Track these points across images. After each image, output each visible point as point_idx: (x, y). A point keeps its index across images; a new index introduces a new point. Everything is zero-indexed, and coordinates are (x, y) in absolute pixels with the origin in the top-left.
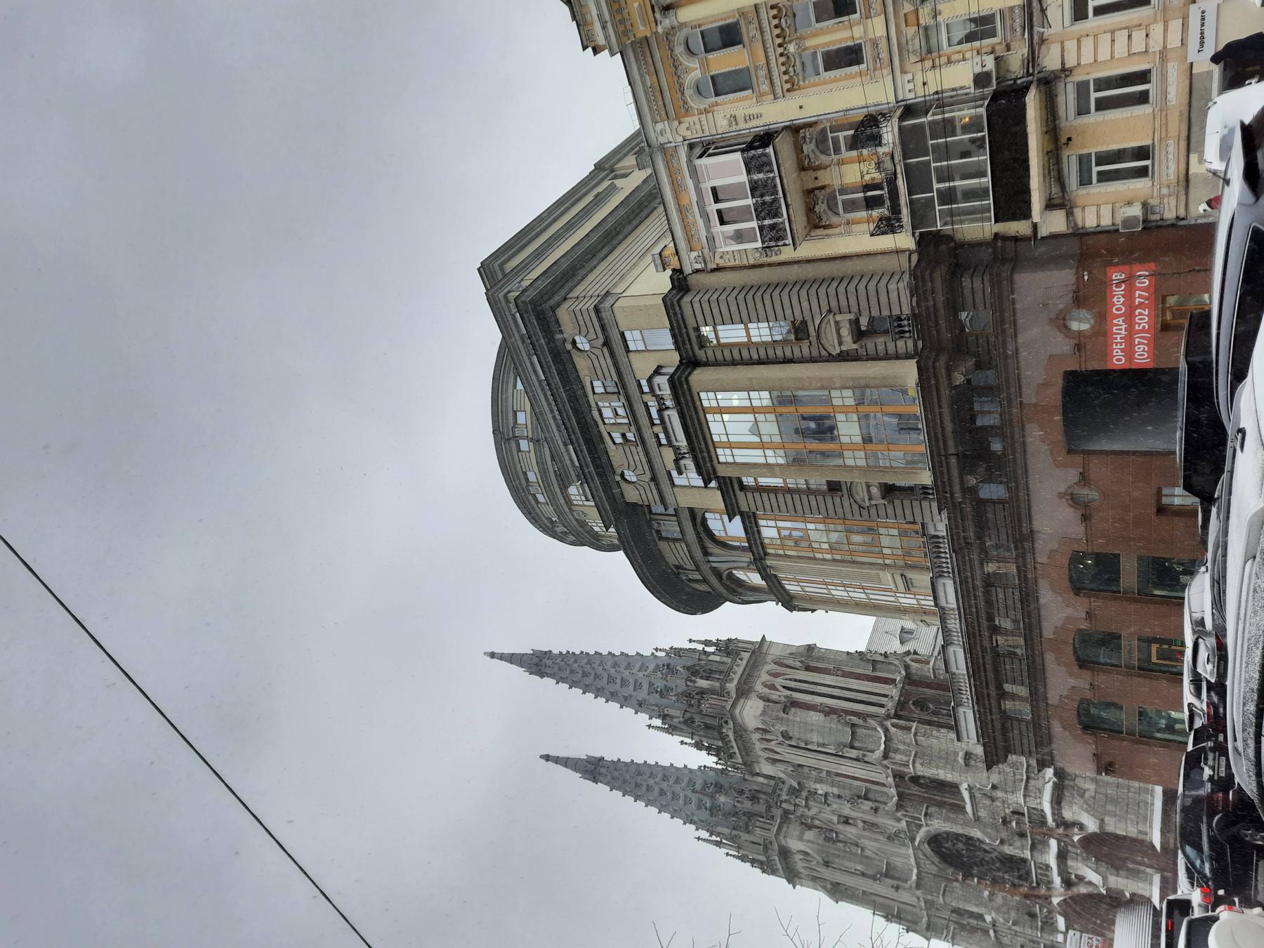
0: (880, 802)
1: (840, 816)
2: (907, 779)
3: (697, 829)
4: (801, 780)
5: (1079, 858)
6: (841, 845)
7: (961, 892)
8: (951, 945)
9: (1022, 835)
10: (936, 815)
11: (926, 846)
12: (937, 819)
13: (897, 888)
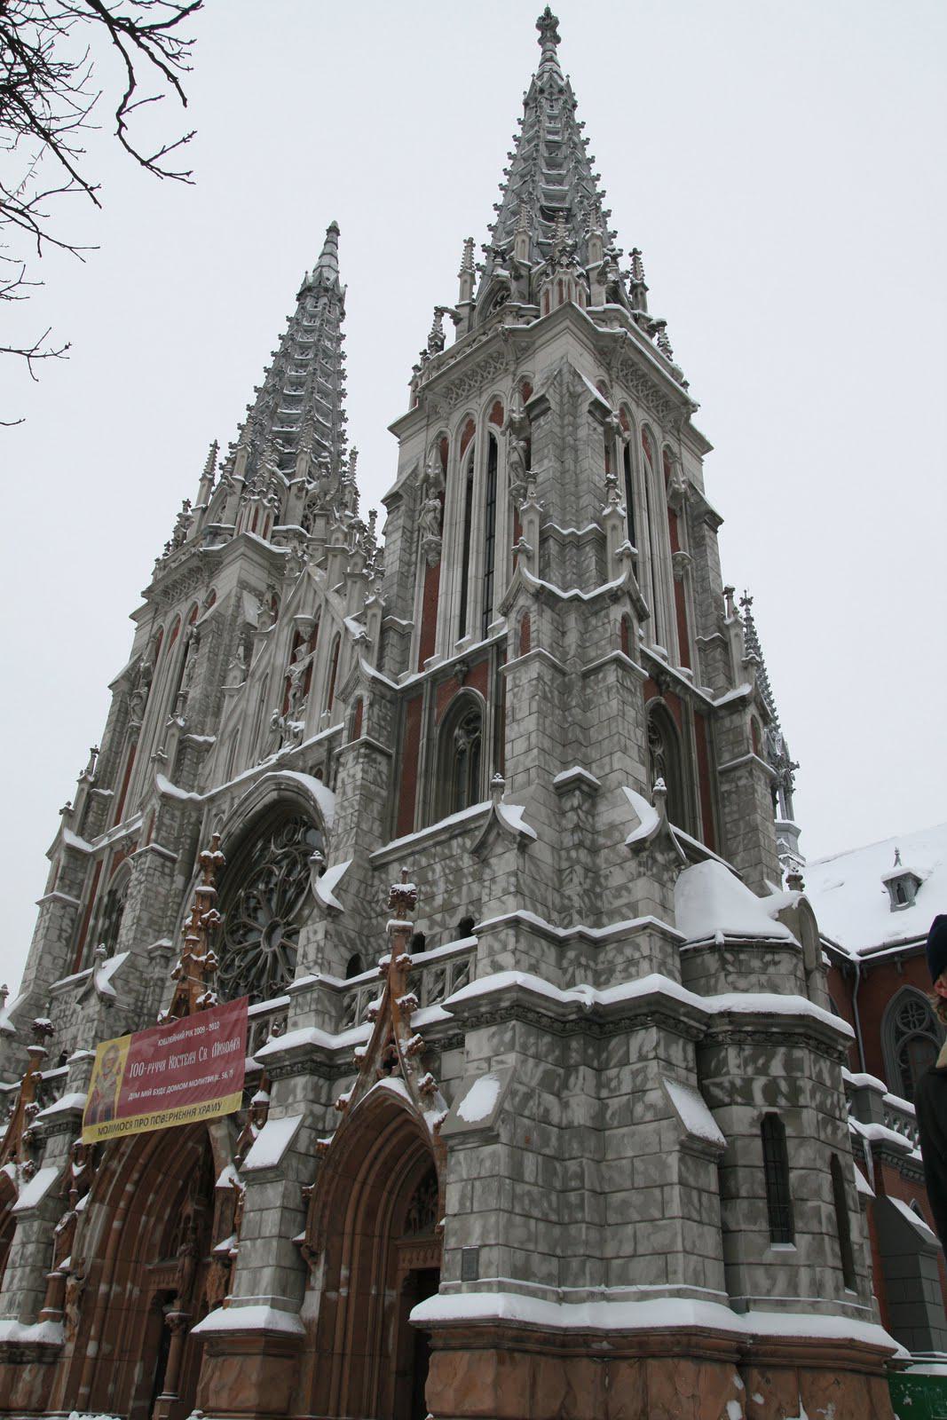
2: (462, 690)
3: (232, 446)
5: (318, 1109)
7: (163, 892)
8: (41, 897)
11: (274, 795)
12: (363, 770)
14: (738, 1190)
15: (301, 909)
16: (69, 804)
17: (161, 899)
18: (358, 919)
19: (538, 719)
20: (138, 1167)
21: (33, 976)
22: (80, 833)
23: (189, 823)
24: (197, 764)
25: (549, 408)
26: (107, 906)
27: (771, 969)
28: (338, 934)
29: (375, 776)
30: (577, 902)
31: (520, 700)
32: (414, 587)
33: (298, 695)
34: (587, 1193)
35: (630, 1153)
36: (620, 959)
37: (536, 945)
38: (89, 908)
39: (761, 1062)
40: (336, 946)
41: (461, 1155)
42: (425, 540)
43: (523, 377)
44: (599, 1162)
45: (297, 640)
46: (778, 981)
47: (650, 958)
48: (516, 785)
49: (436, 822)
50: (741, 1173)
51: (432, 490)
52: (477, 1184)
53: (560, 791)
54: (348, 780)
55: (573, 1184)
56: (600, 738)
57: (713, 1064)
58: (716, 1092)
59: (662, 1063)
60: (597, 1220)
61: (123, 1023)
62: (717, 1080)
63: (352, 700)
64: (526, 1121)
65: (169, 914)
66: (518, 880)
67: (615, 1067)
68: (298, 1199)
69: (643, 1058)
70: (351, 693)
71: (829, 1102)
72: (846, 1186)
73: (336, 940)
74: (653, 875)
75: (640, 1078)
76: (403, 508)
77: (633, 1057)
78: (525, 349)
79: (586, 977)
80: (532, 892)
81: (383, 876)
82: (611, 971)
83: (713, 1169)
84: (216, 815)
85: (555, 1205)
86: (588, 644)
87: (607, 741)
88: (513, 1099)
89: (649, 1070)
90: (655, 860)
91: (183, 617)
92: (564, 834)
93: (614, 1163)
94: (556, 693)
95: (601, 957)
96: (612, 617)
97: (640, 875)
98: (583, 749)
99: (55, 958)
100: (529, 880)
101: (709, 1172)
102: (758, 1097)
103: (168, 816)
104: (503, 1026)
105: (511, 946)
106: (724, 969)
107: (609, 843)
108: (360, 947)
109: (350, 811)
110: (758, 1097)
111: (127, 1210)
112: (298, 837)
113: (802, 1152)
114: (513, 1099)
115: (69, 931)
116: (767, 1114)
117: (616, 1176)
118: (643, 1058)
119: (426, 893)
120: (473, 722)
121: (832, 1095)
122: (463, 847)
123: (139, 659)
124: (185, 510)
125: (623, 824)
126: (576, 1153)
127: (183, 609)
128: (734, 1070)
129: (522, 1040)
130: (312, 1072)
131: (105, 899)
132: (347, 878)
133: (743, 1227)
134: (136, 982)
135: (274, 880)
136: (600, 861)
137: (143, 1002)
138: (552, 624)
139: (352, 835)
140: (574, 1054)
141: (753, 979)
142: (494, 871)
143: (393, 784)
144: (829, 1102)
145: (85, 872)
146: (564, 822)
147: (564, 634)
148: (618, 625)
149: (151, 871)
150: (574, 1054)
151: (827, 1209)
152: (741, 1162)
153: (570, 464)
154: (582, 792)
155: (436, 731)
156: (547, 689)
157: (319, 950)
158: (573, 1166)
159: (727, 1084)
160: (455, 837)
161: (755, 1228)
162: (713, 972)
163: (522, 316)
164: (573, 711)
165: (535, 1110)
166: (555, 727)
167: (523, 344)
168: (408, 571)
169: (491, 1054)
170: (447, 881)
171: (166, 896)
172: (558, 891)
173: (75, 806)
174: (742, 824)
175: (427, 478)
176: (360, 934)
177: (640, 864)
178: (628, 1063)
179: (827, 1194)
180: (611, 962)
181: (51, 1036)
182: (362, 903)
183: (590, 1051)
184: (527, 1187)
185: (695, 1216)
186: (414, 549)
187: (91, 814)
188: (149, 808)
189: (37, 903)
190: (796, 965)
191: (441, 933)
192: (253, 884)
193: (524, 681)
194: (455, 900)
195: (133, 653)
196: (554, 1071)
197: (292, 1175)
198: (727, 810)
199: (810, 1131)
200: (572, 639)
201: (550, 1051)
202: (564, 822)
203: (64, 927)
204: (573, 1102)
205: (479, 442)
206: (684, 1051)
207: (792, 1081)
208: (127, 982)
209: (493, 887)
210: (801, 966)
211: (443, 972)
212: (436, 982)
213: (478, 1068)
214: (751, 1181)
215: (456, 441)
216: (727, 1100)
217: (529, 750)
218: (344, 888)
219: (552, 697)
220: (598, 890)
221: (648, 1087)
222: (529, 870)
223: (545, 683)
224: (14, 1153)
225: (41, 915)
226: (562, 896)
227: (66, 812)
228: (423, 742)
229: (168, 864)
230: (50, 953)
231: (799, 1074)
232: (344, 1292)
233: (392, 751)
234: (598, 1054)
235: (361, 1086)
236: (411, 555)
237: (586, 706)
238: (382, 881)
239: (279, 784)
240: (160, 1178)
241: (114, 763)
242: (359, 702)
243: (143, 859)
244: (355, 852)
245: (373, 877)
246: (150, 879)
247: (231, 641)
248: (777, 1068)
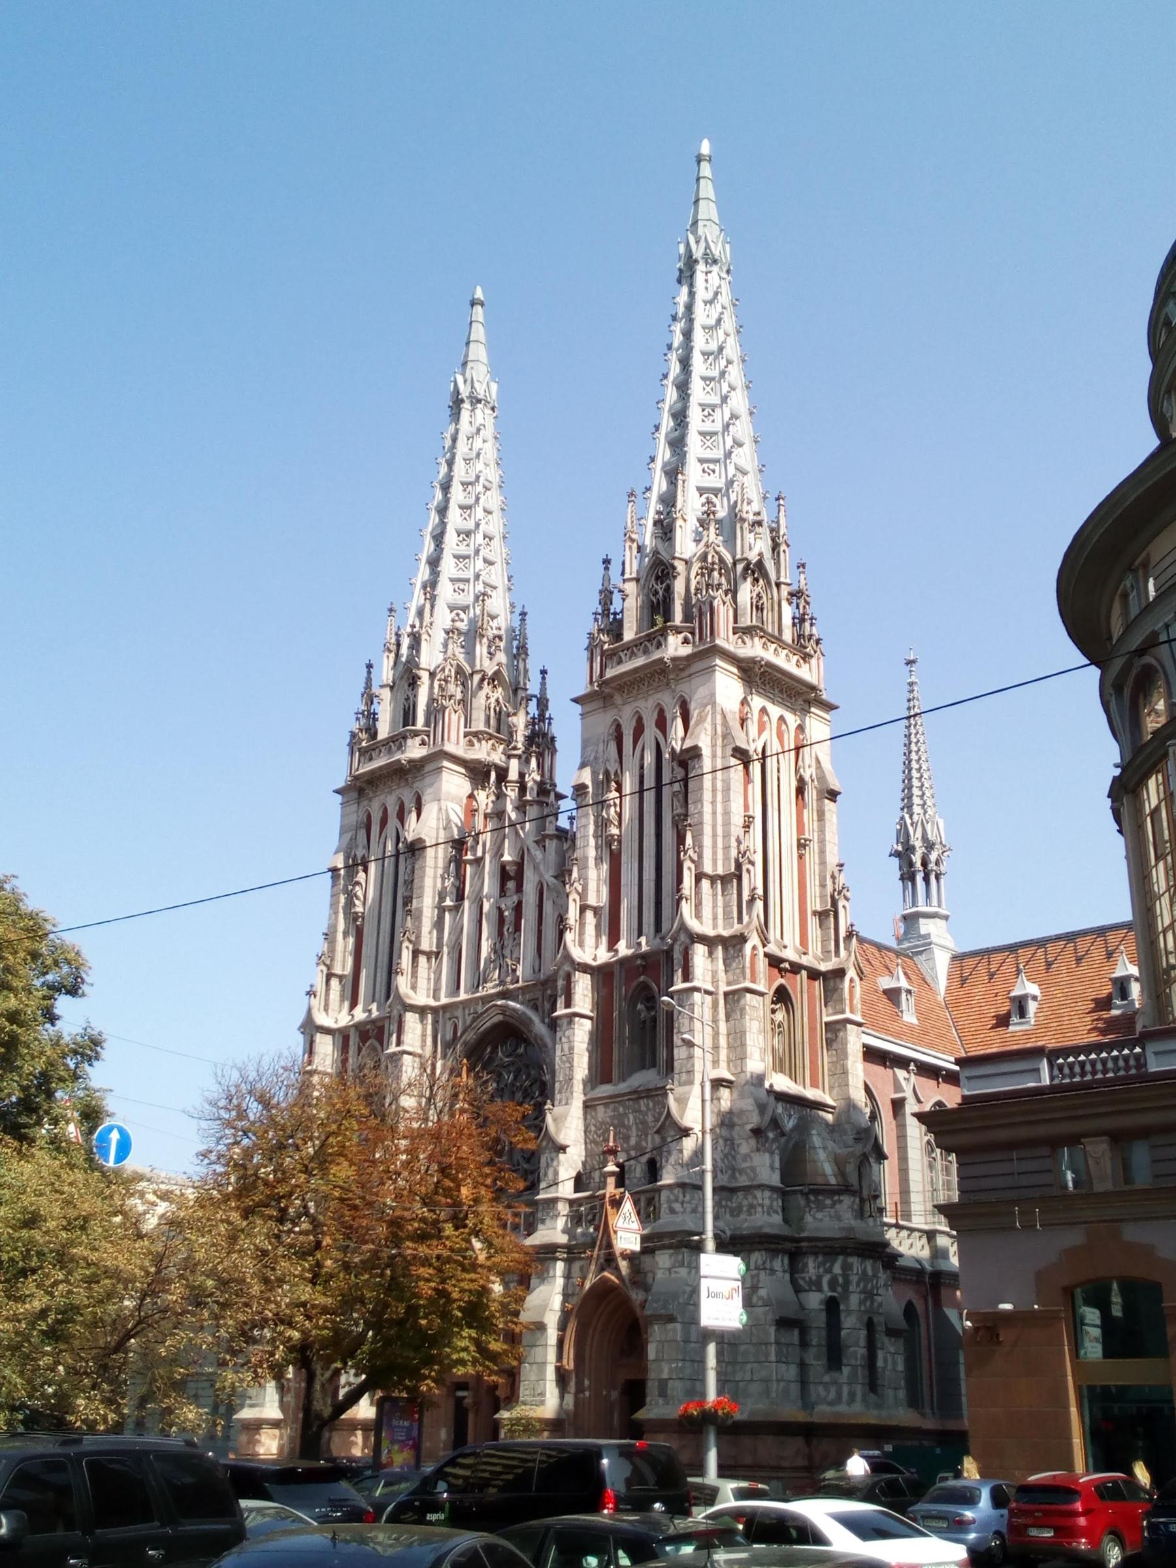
2: (642, 978)
11: (500, 1017)
27: (838, 1206)
36: (745, 1203)
37: (696, 1195)
50: (814, 1332)
52: (666, 1344)
58: (801, 1282)
62: (803, 1275)
69: (757, 1268)
81: (593, 1114)
83: (796, 1332)
90: (767, 1138)
102: (825, 1287)
107: (740, 1122)
110: (825, 1287)
112: (521, 1050)
122: (648, 1109)
136: (735, 1134)
144: (869, 1286)
151: (862, 1351)
152: (814, 1325)
159: (807, 1279)
170: (638, 1129)
177: (758, 1143)
179: (863, 1342)
180: (741, 1203)
184: (692, 1345)
190: (854, 1202)
210: (857, 1200)
214: (817, 1337)
216: (807, 1288)
221: (760, 1285)
232: (587, 1394)
238: (593, 1117)
239: (504, 1008)
248: (837, 1269)
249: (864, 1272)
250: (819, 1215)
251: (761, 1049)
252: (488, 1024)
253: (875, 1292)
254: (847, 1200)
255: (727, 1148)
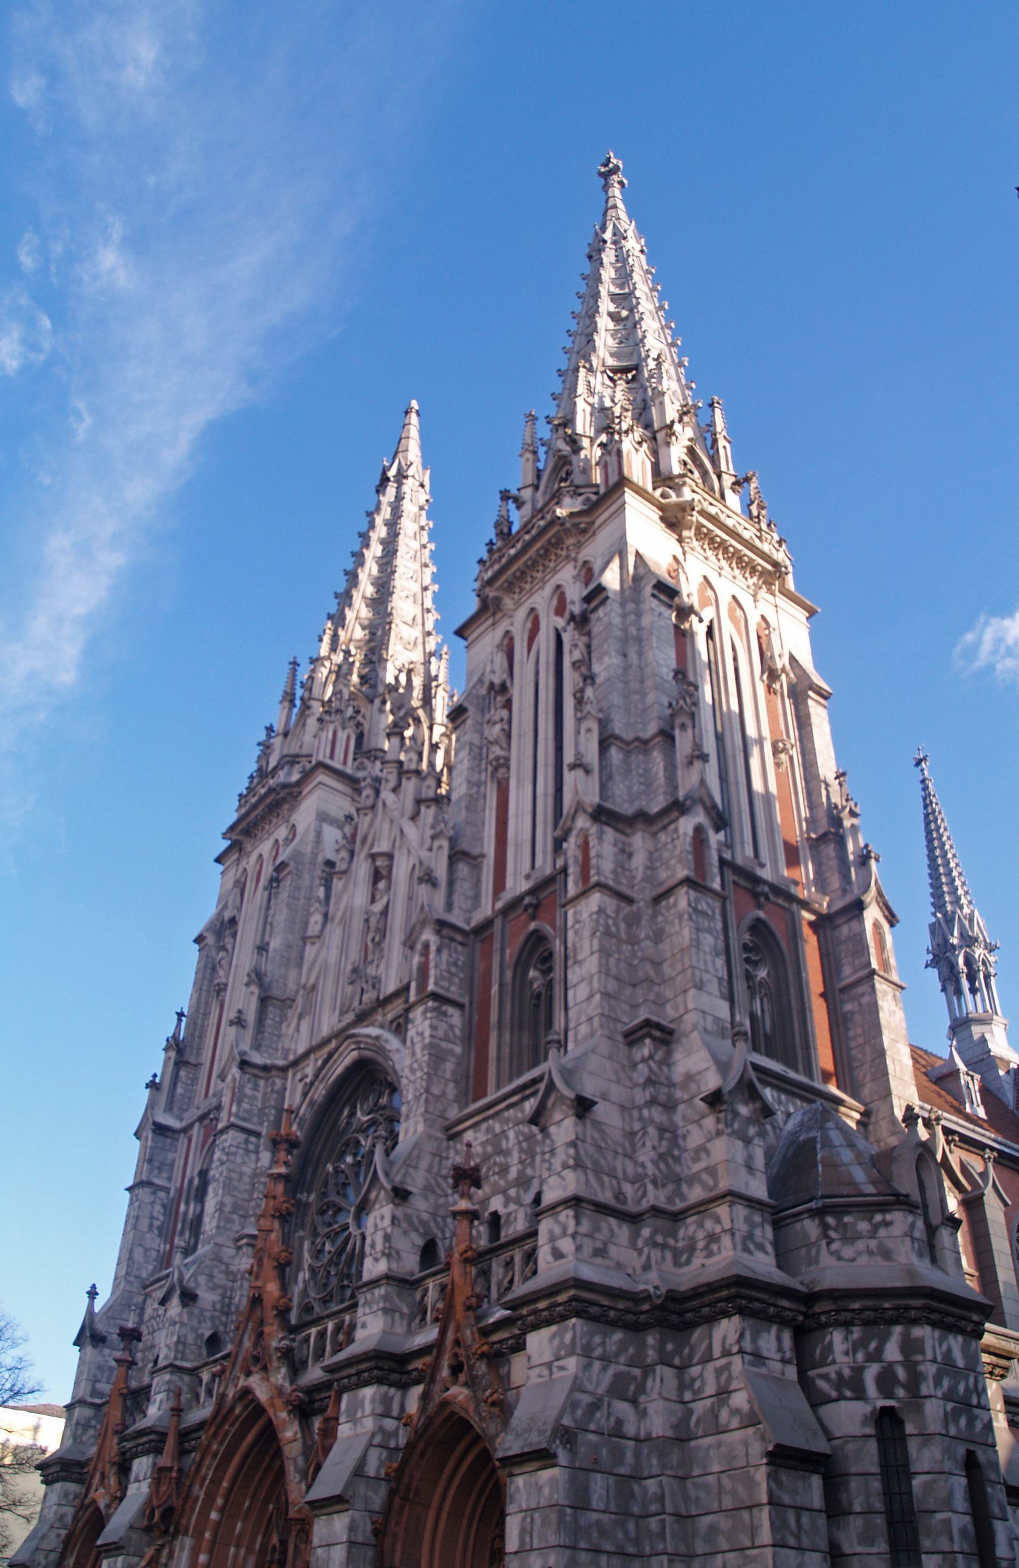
0: (450, 894)
1: (390, 856)
2: (533, 926)
4: (472, 712)
5: (390, 1424)
6: (321, 892)
7: (247, 1170)
8: (130, 1183)
9: (428, 1252)
10: (443, 1026)
11: (355, 1054)
12: (433, 1027)
13: (239, 1022)
14: (851, 1504)
15: (368, 1191)
16: (155, 1076)
17: (246, 1179)
18: (432, 1198)
19: (600, 958)
20: (222, 1491)
21: (123, 1272)
22: (169, 1108)
23: (272, 1091)
24: (281, 1023)
25: (607, 598)
26: (197, 1189)
27: (882, 1232)
28: (408, 1218)
29: (446, 1032)
30: (650, 1169)
31: (581, 939)
32: (484, 810)
33: (377, 939)
34: (668, 1519)
35: (716, 1468)
37: (603, 1225)
38: (180, 1190)
39: (873, 1345)
40: (405, 1233)
41: (520, 1481)
42: (491, 756)
43: (586, 562)
44: (684, 1479)
45: (377, 876)
46: (890, 1245)
47: (732, 1232)
48: (580, 1037)
49: (510, 1080)
50: (854, 1484)
51: (499, 698)
52: (536, 1515)
53: (631, 1038)
54: (417, 1039)
55: (654, 1508)
56: (674, 973)
57: (818, 1351)
58: (822, 1384)
59: (747, 1357)
60: (682, 1549)
61: (209, 1324)
63: (419, 946)
64: (592, 1437)
65: (255, 1195)
66: (577, 1152)
67: (697, 1364)
68: (369, 1534)
69: (726, 1353)
70: (417, 938)
71: (961, 1387)
72: (989, 1490)
73: (404, 1225)
74: (733, 1132)
75: (724, 1377)
76: (469, 722)
77: (717, 1351)
78: (584, 531)
79: (663, 1258)
80: (596, 1163)
82: (691, 1249)
83: (816, 1481)
84: (301, 1080)
85: (633, 1534)
86: (658, 864)
87: (679, 978)
88: (573, 1413)
89: (733, 1367)
90: (736, 1114)
91: (265, 856)
92: (635, 1091)
93: (701, 1480)
94: (622, 925)
95: (681, 1233)
96: (681, 832)
97: (719, 1133)
98: (656, 988)
99: (146, 1250)
100: (591, 1150)
101: (810, 1484)
103: (249, 1086)
104: (563, 1324)
105: (571, 1230)
106: (827, 1236)
107: (686, 1097)
108: (435, 1230)
109: (419, 1074)
111: (213, 1542)
112: (384, 1101)
113: (927, 1453)
114: (573, 1413)
115: (162, 1218)
116: (883, 1408)
117: (702, 1495)
118: (726, 1353)
119: (500, 1165)
120: (546, 961)
121: (966, 1378)
123: (225, 907)
124: (269, 736)
125: (699, 1073)
126: (655, 1470)
127: (265, 848)
128: (840, 1358)
129: (584, 1341)
130: (380, 1381)
131: (196, 1181)
132: (416, 1153)
133: (858, 1549)
134: (223, 1276)
135: (362, 1151)
136: (678, 1119)
137: (231, 1298)
138: (615, 845)
139: (422, 1101)
140: (650, 1352)
141: (861, 1245)
142: (553, 1141)
143: (467, 1040)
144: (961, 1387)
145: (176, 1151)
146: (635, 1076)
147: (630, 855)
148: (688, 840)
149: (233, 1150)
150: (650, 1352)
151: (961, 1521)
152: (854, 1469)
153: (633, 658)
154: (654, 1039)
155: (509, 974)
156: (610, 922)
157: (387, 1238)
158: (652, 1485)
159: (833, 1376)
160: (526, 1098)
161: (874, 1550)
162: (813, 1240)
163: (580, 495)
164: (643, 944)
165: (603, 1421)
166: (622, 965)
167: (583, 526)
168: (478, 792)
169: (552, 1358)
170: (521, 1150)
171: (255, 1175)
172: (630, 1158)
173: (162, 1079)
174: (868, 1049)
175: (492, 685)
176: (434, 1215)
177: (718, 1121)
178: (710, 1359)
179: (960, 1502)
181: (139, 1340)
182: (436, 1180)
183: (670, 1347)
184: (595, 1516)
185: (792, 1541)
186: (483, 766)
187: (179, 1085)
188: (229, 1078)
189: (128, 1189)
190: (912, 1226)
191: (516, 1211)
192: (342, 1155)
193: (585, 915)
194: (529, 1172)
195: (219, 902)
196: (628, 1373)
197: (359, 1504)
198: (851, 1033)
199: (934, 1426)
200: (639, 861)
201: (622, 1348)
202: (635, 1076)
203: (155, 1214)
204: (651, 1408)
205: (545, 641)
206: (779, 1339)
207: (911, 1366)
208: (211, 1277)
209: (553, 1161)
210: (920, 1224)
211: (512, 1258)
212: (506, 1274)
213: (540, 1376)
215: (522, 640)
216: (834, 1394)
217: (590, 997)
218: (414, 1163)
219: (618, 930)
220: (676, 1153)
222: (593, 1138)
223: (608, 916)
224: (103, 1476)
225: (131, 1204)
226: (636, 1163)
227: (152, 1085)
228: (495, 988)
229: (253, 1139)
230: (141, 1245)
231: (919, 1358)
233: (465, 1000)
234: (678, 1351)
235: (425, 1397)
236: (480, 773)
237: (658, 937)
240: (247, 1503)
241: (203, 1026)
242: (426, 946)
243: (224, 1137)
244: (425, 1120)
245: (448, 1148)
246: (231, 1158)
247: (312, 882)
248: (892, 1352)
249: (948, 1360)
250: (848, 1252)
251: (720, 979)
252: (340, 1070)
253: (975, 1401)
254: (899, 1220)
255: (665, 1143)
